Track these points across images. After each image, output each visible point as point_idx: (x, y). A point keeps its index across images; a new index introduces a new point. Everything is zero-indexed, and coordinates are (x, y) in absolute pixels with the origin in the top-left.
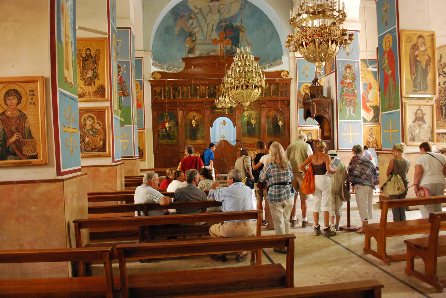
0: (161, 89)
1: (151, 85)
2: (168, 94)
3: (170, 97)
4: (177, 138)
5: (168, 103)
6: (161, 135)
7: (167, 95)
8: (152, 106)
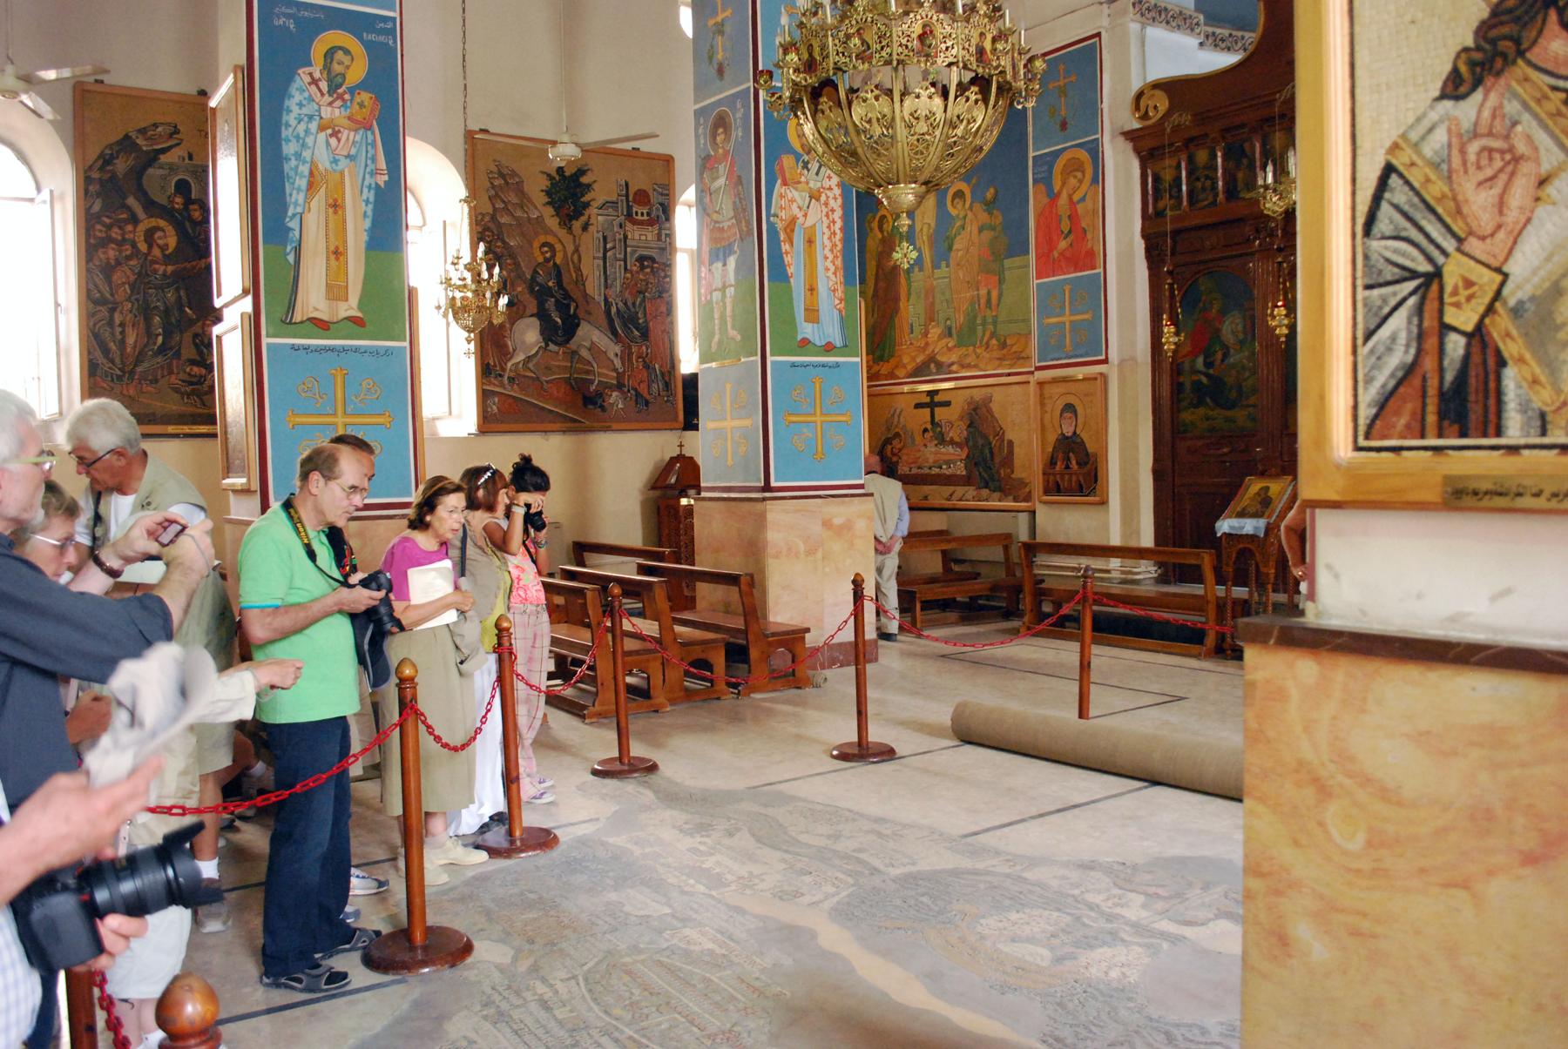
0: (1178, 166)
1: (1137, 151)
2: (1208, 183)
3: (1217, 195)
4: (1252, 400)
5: (1175, 233)
6: (1188, 386)
7: (1204, 189)
8: (1148, 250)
